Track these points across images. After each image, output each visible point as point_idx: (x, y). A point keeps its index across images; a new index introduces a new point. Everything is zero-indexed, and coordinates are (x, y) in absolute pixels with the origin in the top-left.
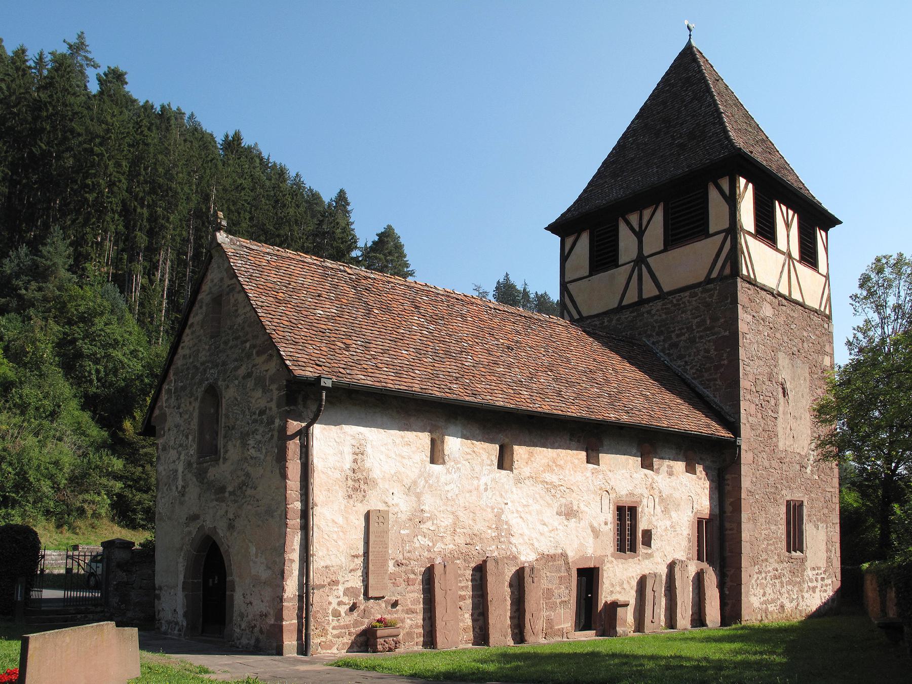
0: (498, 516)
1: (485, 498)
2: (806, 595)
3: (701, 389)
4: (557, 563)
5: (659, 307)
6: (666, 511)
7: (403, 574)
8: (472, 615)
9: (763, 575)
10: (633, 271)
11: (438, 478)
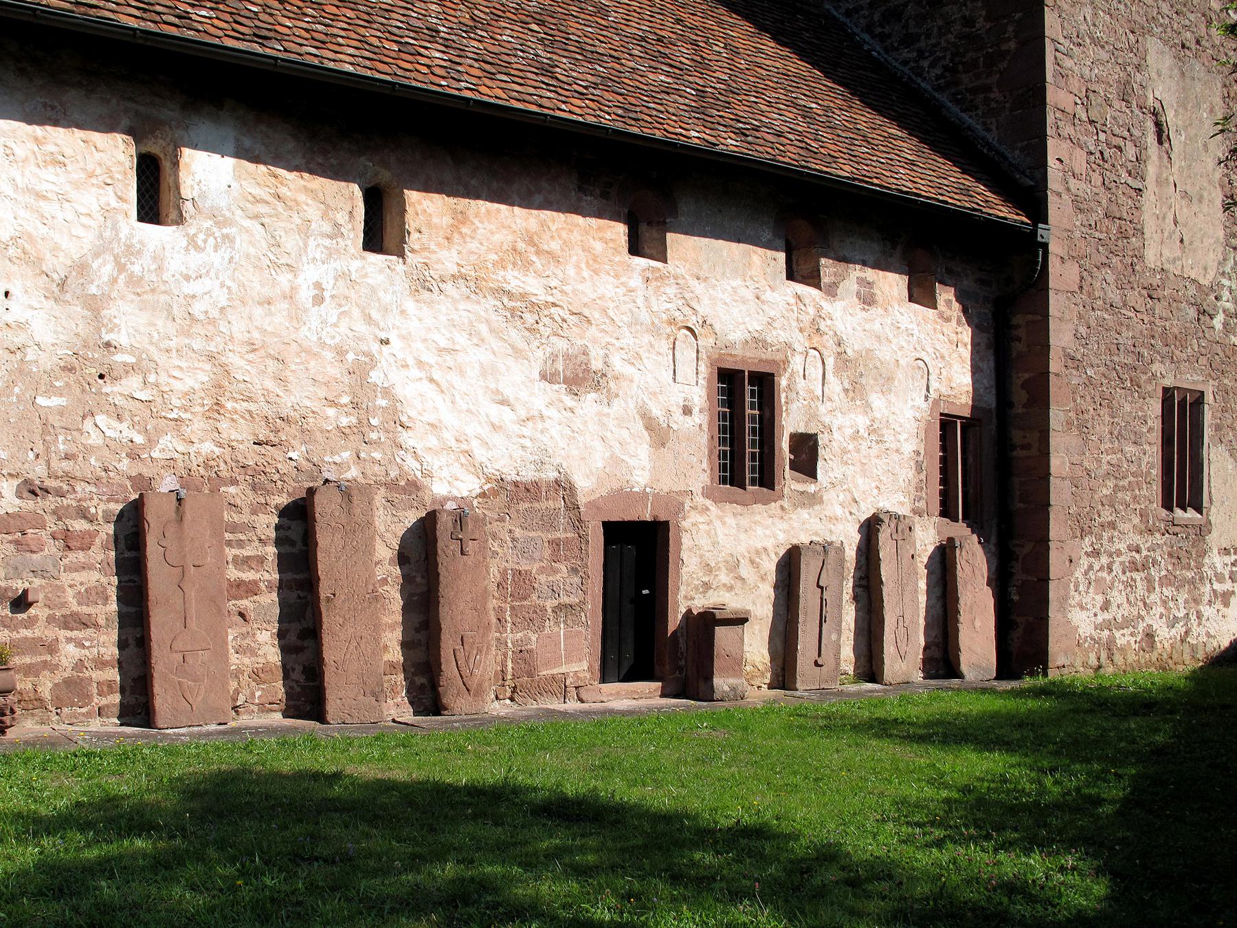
0: (359, 372)
1: (314, 323)
2: (1207, 611)
4: (543, 505)
6: (855, 390)
7: (50, 520)
8: (281, 635)
9: (1104, 560)
11: (159, 259)
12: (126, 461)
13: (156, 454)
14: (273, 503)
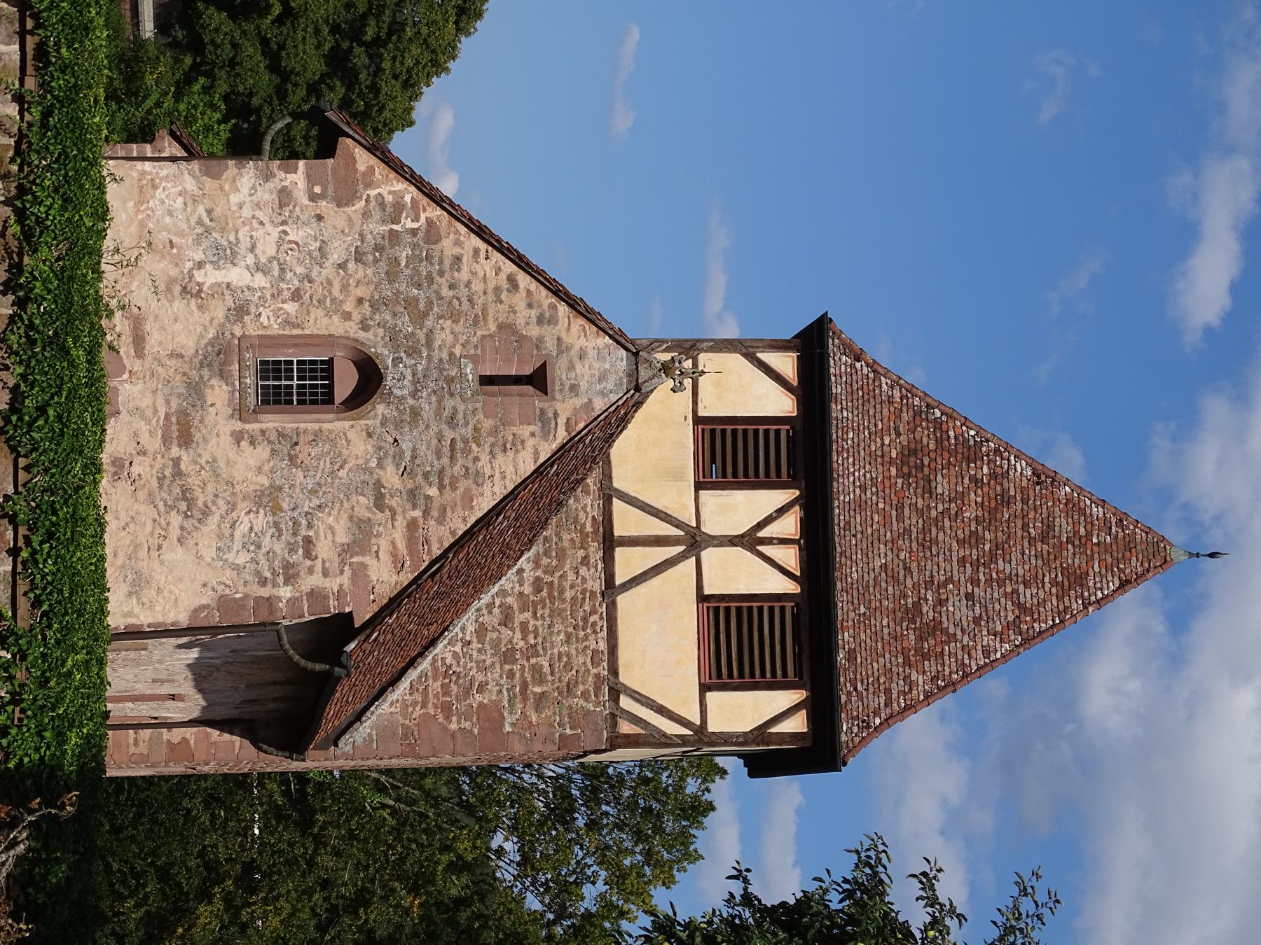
3: (413, 674)
5: (589, 585)
10: (677, 524)
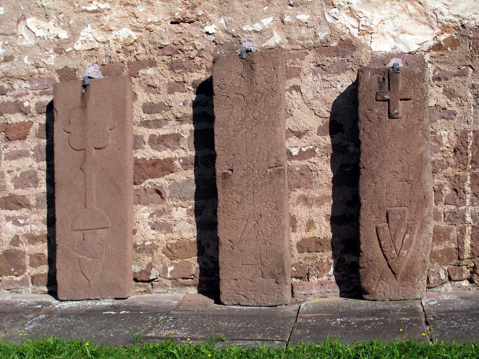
12: (53, 57)
13: (78, 46)
14: (190, 80)
